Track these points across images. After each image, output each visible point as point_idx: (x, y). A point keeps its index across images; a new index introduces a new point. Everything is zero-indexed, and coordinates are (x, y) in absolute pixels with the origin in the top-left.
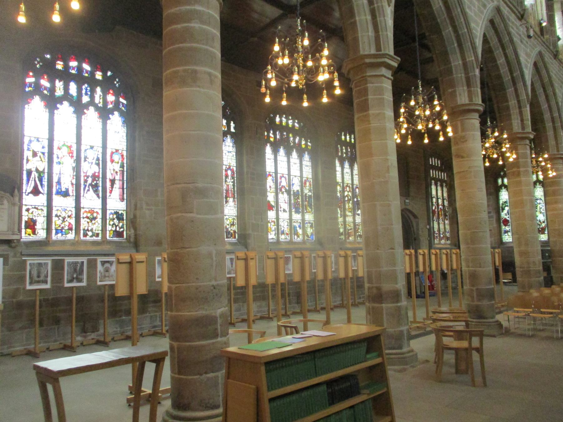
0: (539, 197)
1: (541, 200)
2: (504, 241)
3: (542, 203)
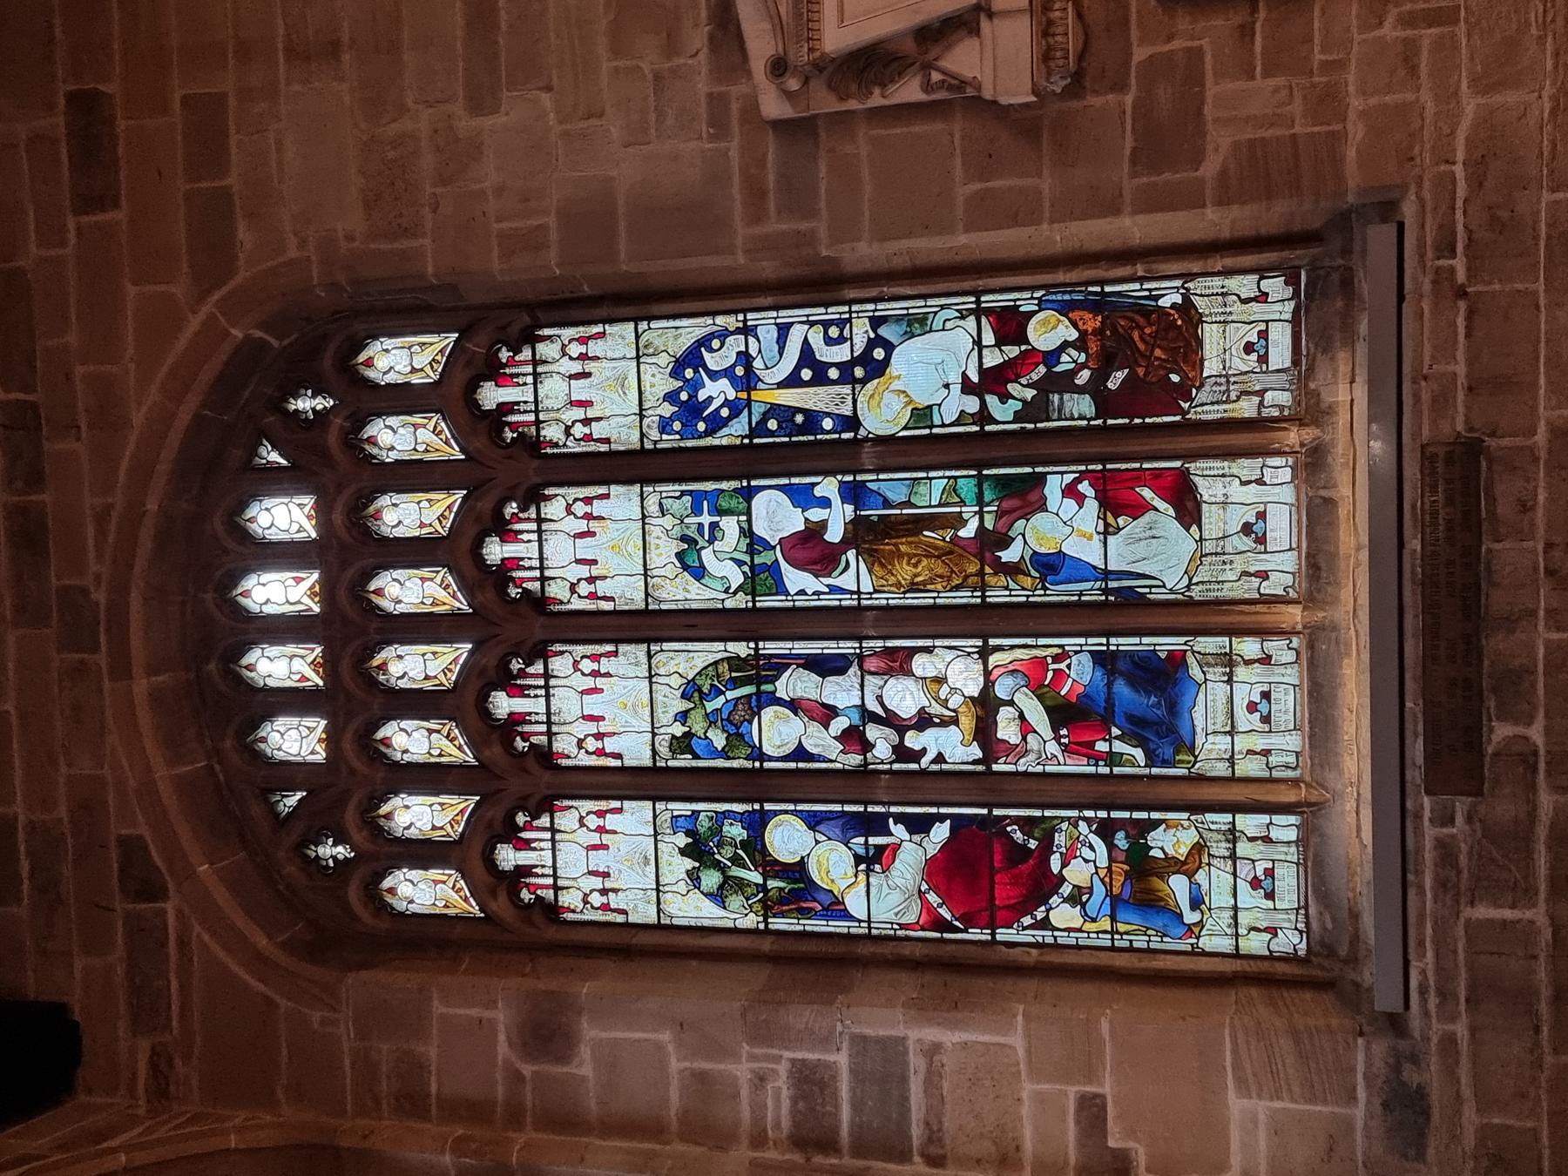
0: (659, 382)
1: (691, 359)
2: (1290, 941)
3: (735, 344)
